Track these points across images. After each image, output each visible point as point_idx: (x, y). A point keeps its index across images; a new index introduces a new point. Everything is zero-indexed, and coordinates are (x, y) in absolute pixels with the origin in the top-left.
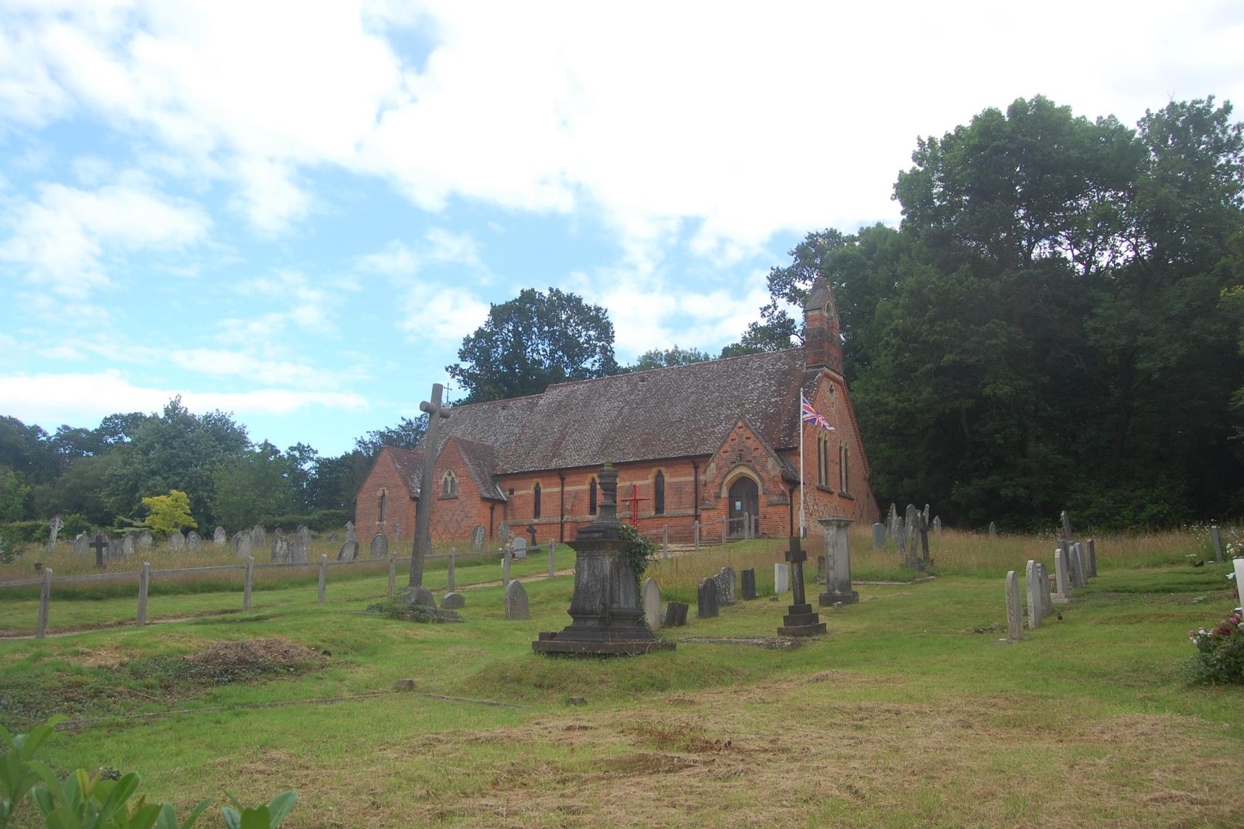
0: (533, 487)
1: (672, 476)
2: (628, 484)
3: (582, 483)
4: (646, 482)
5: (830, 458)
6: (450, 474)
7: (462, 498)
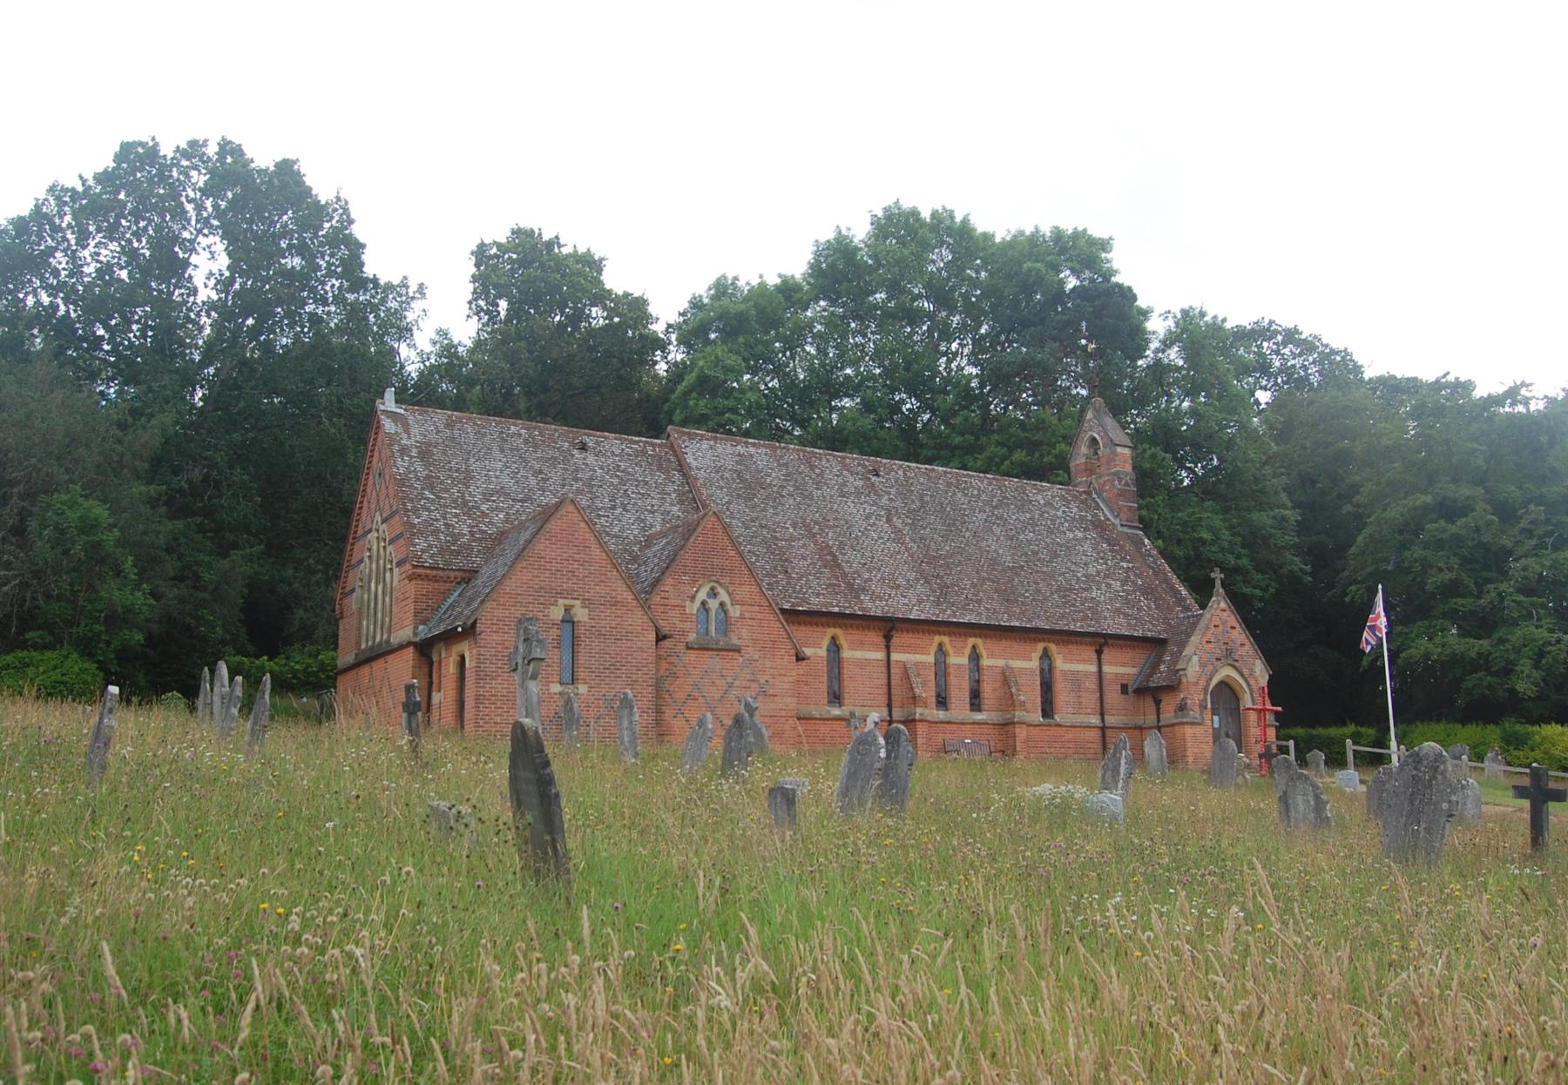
0: (826, 642)
1: (1065, 660)
2: (1001, 663)
3: (922, 650)
4: (1026, 663)
6: (713, 594)
7: (750, 652)
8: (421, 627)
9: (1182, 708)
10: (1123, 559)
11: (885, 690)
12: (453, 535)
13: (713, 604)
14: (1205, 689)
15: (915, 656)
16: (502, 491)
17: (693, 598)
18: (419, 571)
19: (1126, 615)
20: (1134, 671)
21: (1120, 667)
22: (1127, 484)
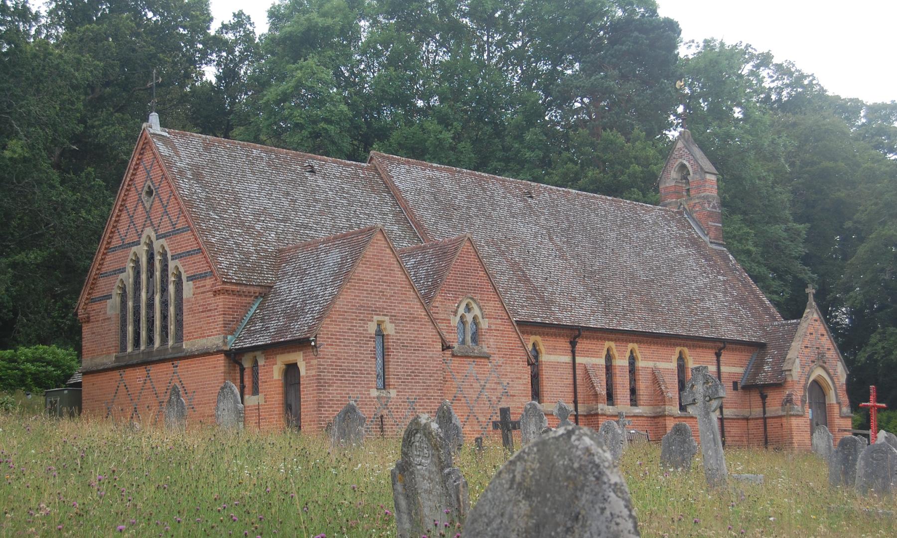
2: (651, 364)
3: (595, 355)
6: (468, 309)
7: (497, 359)
8: (229, 337)
9: (789, 401)
10: (718, 273)
11: (571, 388)
12: (244, 254)
13: (469, 318)
14: (805, 386)
15: (592, 359)
16: (264, 211)
17: (455, 313)
18: (227, 287)
19: (734, 323)
20: (740, 370)
21: (733, 367)
22: (714, 207)
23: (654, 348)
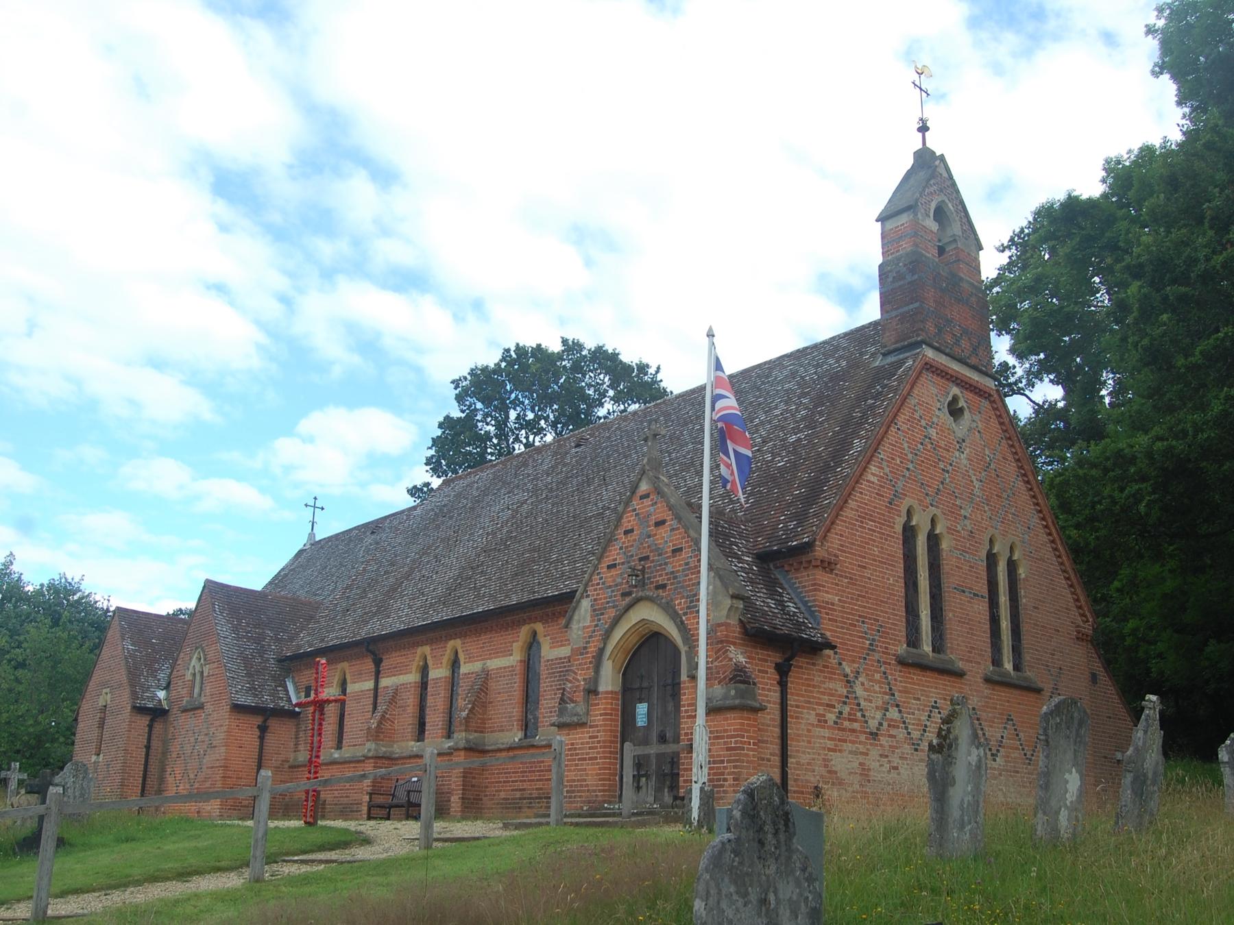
2: (476, 666)
5: (949, 581)
7: (209, 708)
23: (484, 638)
